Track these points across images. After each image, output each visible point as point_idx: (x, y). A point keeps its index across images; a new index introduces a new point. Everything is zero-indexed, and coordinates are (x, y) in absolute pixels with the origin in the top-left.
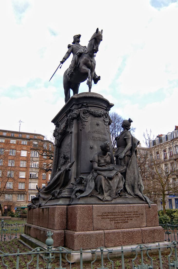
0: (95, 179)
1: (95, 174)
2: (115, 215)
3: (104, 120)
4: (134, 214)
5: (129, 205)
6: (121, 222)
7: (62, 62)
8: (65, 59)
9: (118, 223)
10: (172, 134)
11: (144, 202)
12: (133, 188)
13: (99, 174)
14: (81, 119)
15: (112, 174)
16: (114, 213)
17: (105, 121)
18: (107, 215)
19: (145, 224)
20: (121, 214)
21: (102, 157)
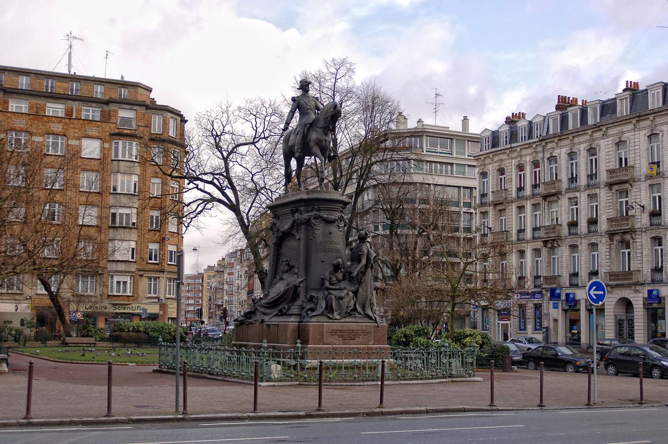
0: (326, 298)
1: (326, 293)
3: (338, 225)
11: (373, 321)
12: (364, 307)
13: (329, 294)
15: (343, 294)
17: (339, 227)
18: (336, 333)
19: (372, 342)
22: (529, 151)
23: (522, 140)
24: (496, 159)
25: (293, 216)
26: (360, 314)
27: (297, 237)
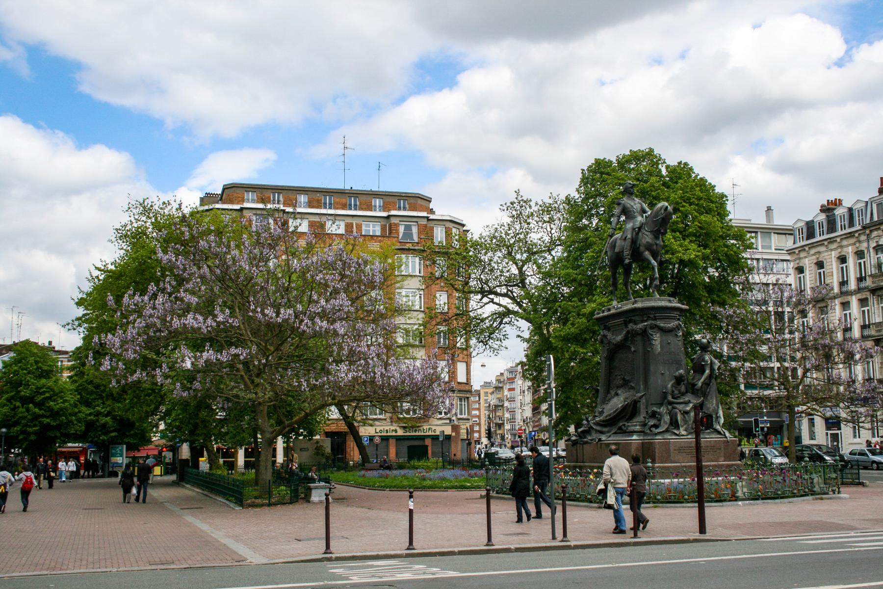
0: (670, 413)
1: (670, 407)
10: (867, 205)
13: (674, 408)
14: (648, 336)
22: (852, 241)
23: (842, 230)
24: (813, 251)
25: (626, 326)
27: (633, 349)
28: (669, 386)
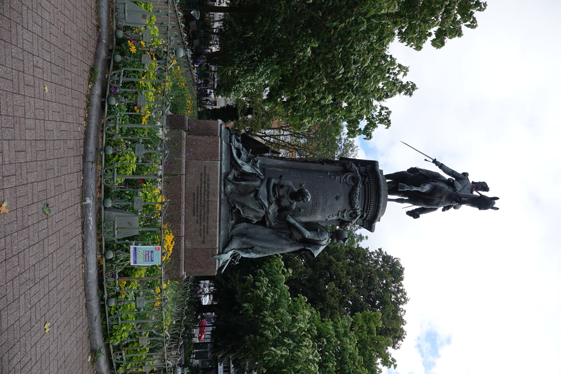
2: (205, 194)
3: (345, 210)
4: (204, 226)
5: (218, 220)
6: (194, 204)
7: (435, 161)
8: (441, 166)
9: (194, 199)
11: (221, 250)
12: (241, 235)
16: (208, 195)
17: (344, 212)
19: (189, 246)
20: (206, 204)
21: (288, 192)
26: (233, 228)
28: (290, 183)
